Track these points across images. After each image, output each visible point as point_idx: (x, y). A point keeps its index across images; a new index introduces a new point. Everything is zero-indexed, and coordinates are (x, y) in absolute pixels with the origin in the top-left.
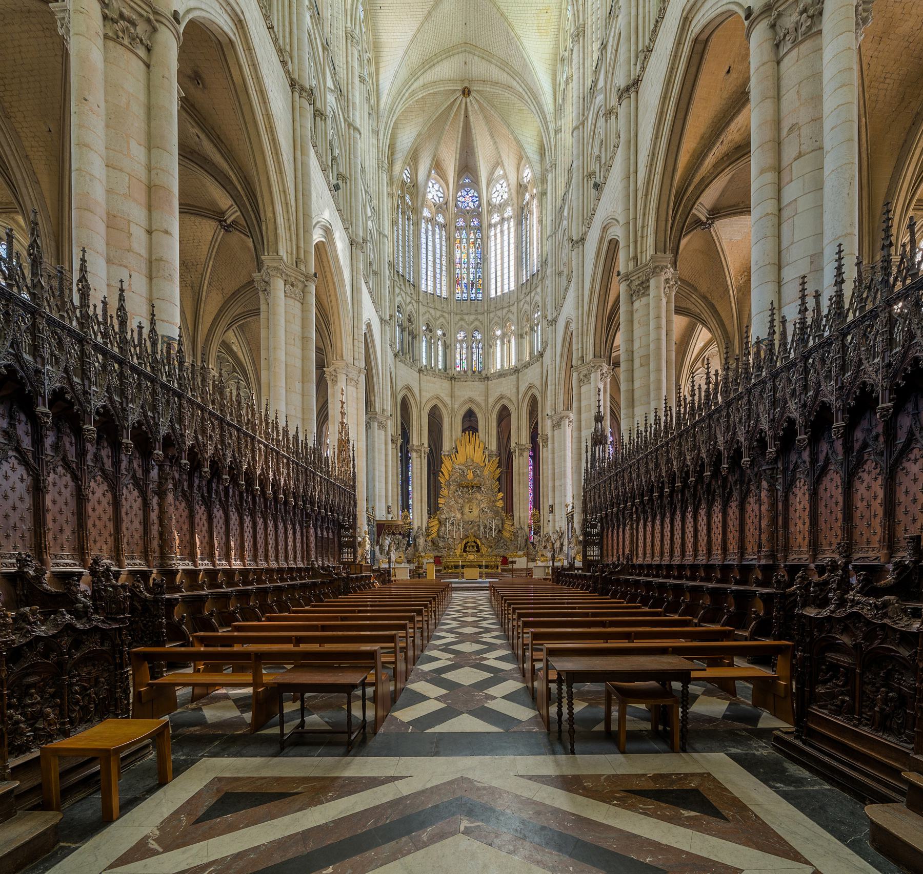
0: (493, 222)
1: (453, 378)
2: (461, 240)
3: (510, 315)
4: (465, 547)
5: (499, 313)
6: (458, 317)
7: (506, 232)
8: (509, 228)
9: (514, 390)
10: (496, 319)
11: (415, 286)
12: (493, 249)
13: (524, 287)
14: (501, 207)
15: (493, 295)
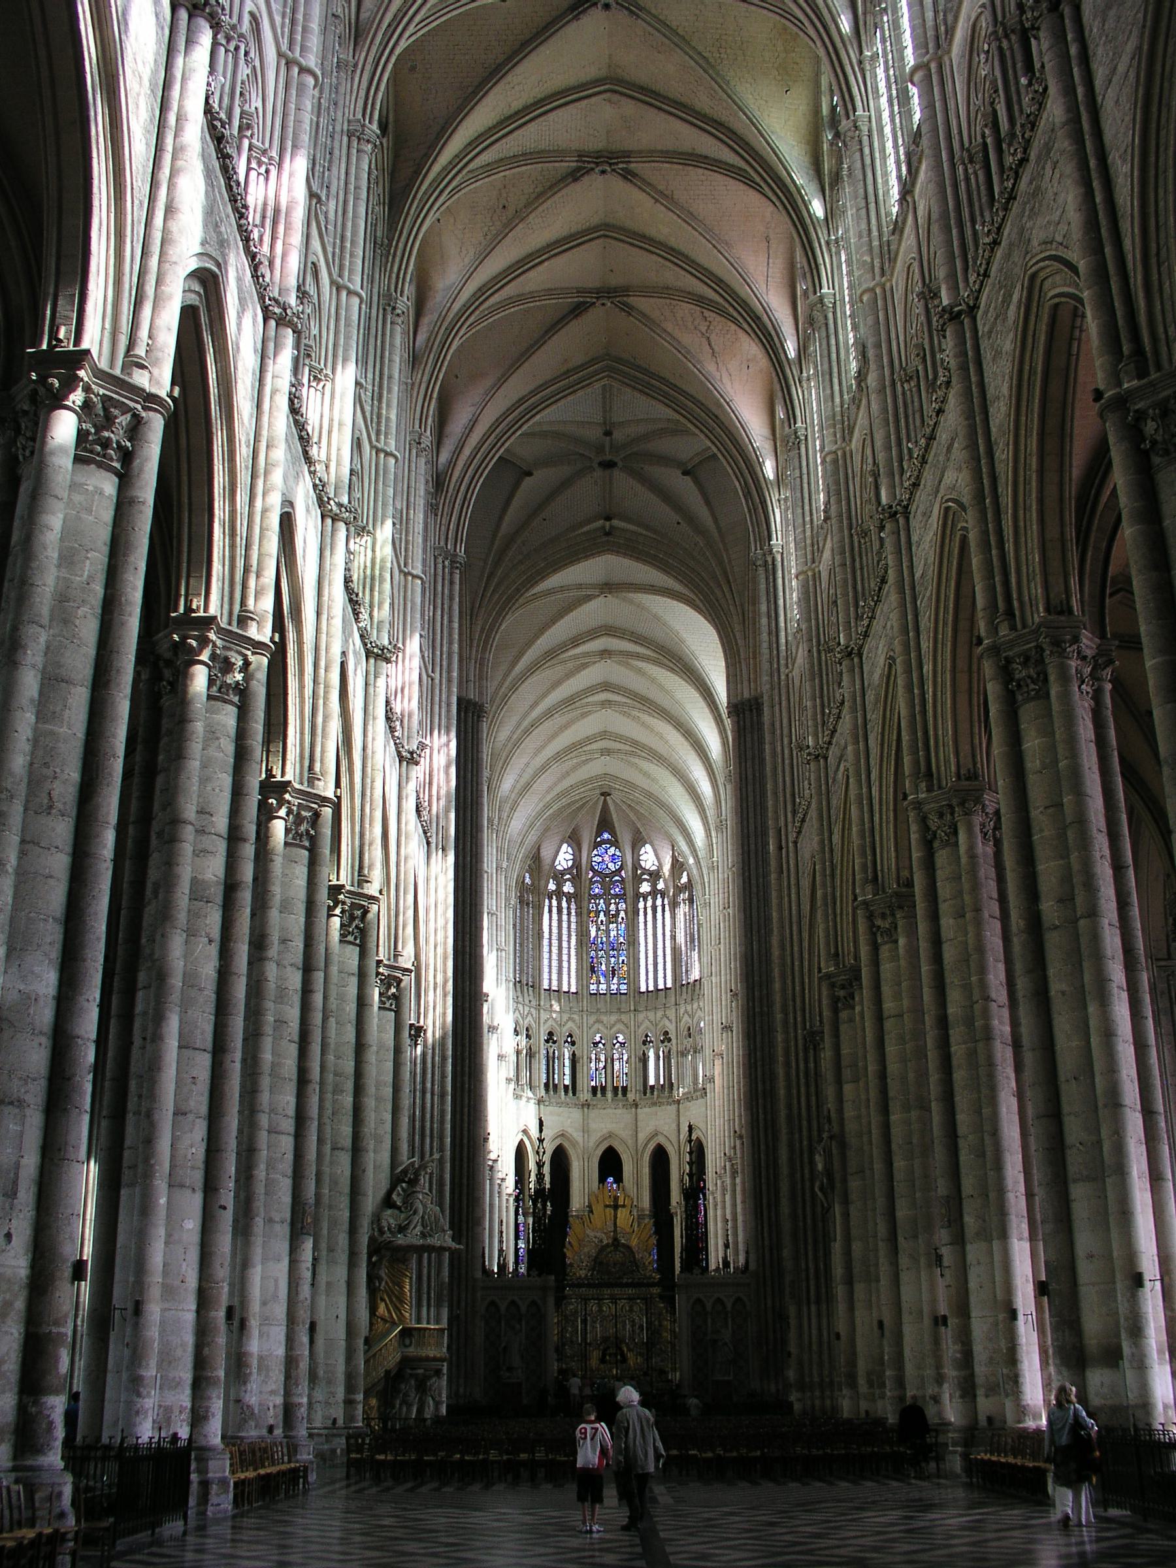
0: (641, 890)
1: (586, 1105)
2: (597, 913)
3: (667, 1023)
4: (604, 1355)
5: (651, 1015)
6: (592, 1019)
7: (659, 909)
8: (663, 906)
9: (674, 1126)
10: (647, 1023)
11: (535, 986)
12: (642, 926)
13: (684, 988)
14: (655, 876)
15: (643, 989)
